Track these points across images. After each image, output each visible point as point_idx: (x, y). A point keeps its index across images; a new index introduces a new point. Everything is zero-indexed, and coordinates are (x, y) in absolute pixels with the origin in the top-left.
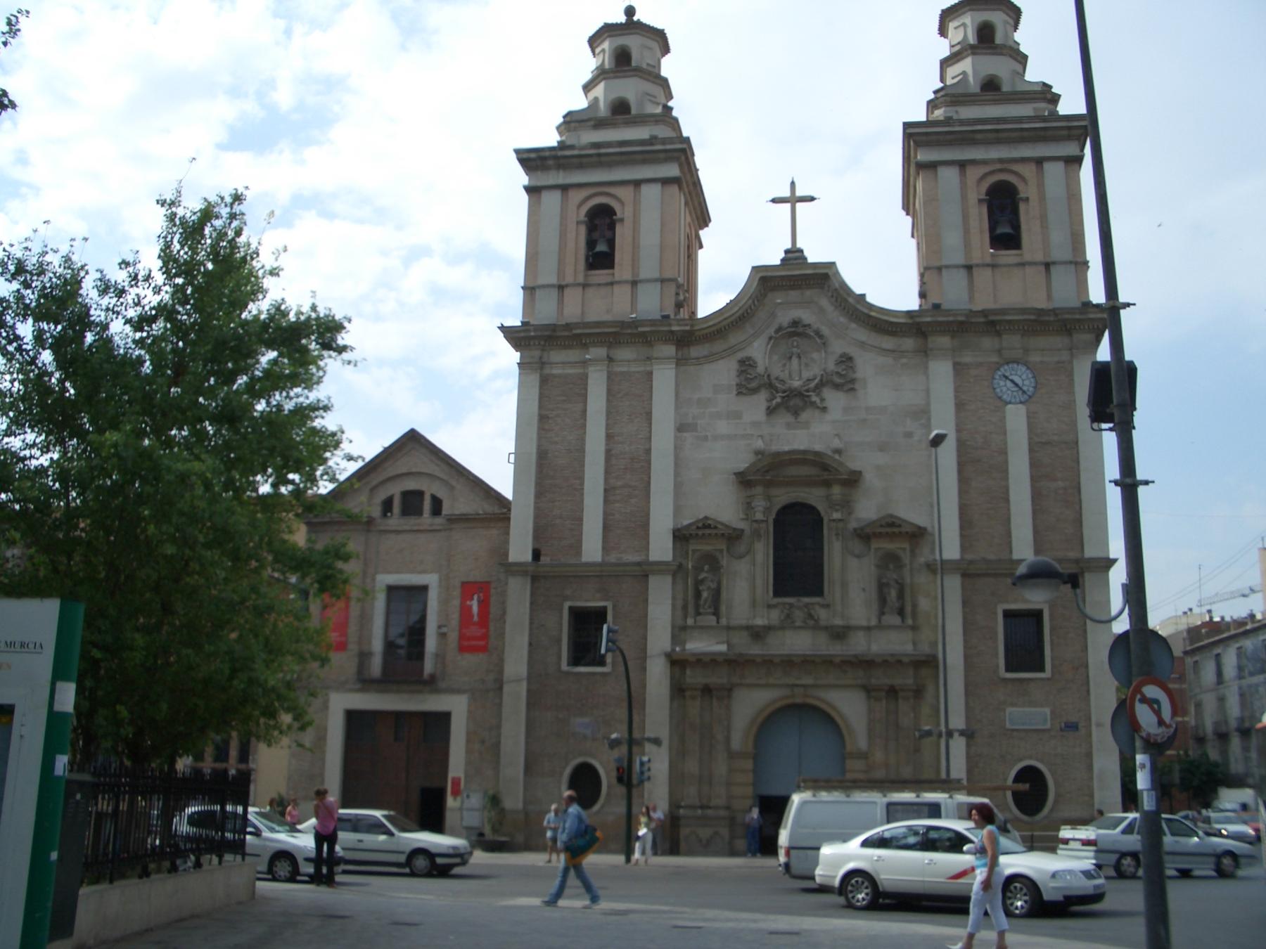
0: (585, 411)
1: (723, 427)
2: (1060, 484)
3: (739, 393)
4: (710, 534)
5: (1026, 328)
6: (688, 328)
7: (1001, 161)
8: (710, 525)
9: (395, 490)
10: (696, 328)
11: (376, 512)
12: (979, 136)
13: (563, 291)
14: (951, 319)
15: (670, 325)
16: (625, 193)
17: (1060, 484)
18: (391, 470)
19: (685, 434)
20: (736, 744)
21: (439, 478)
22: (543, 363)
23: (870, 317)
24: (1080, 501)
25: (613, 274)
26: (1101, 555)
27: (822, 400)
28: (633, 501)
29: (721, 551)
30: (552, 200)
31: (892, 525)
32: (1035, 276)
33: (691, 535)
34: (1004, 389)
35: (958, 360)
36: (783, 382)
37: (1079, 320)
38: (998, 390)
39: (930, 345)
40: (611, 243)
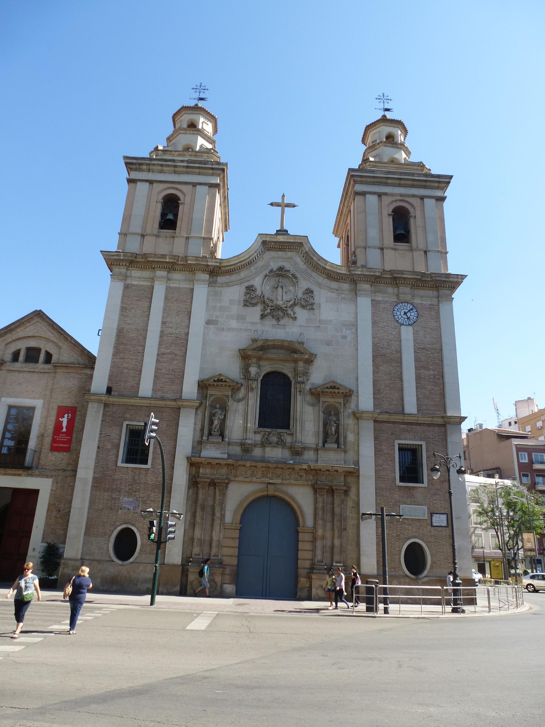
0: (150, 307)
1: (234, 324)
2: (431, 372)
3: (245, 305)
4: (222, 385)
5: (413, 283)
6: (218, 264)
7: (401, 195)
8: (222, 379)
9: (23, 346)
10: (223, 265)
11: (8, 357)
12: (390, 181)
13: (144, 238)
14: (372, 274)
15: (208, 261)
16: (186, 189)
17: (431, 372)
18: (21, 332)
19: (210, 326)
20: (228, 518)
21: (52, 341)
22: (126, 277)
23: (325, 268)
24: (443, 383)
25: (175, 233)
26: (456, 415)
27: (294, 313)
28: (175, 362)
29: (228, 396)
30: (142, 188)
31: (334, 388)
32: (418, 256)
33: (209, 385)
34: (400, 317)
35: (374, 298)
36: (272, 301)
37: (444, 281)
38: (396, 317)
39: (358, 288)
40: (176, 215)
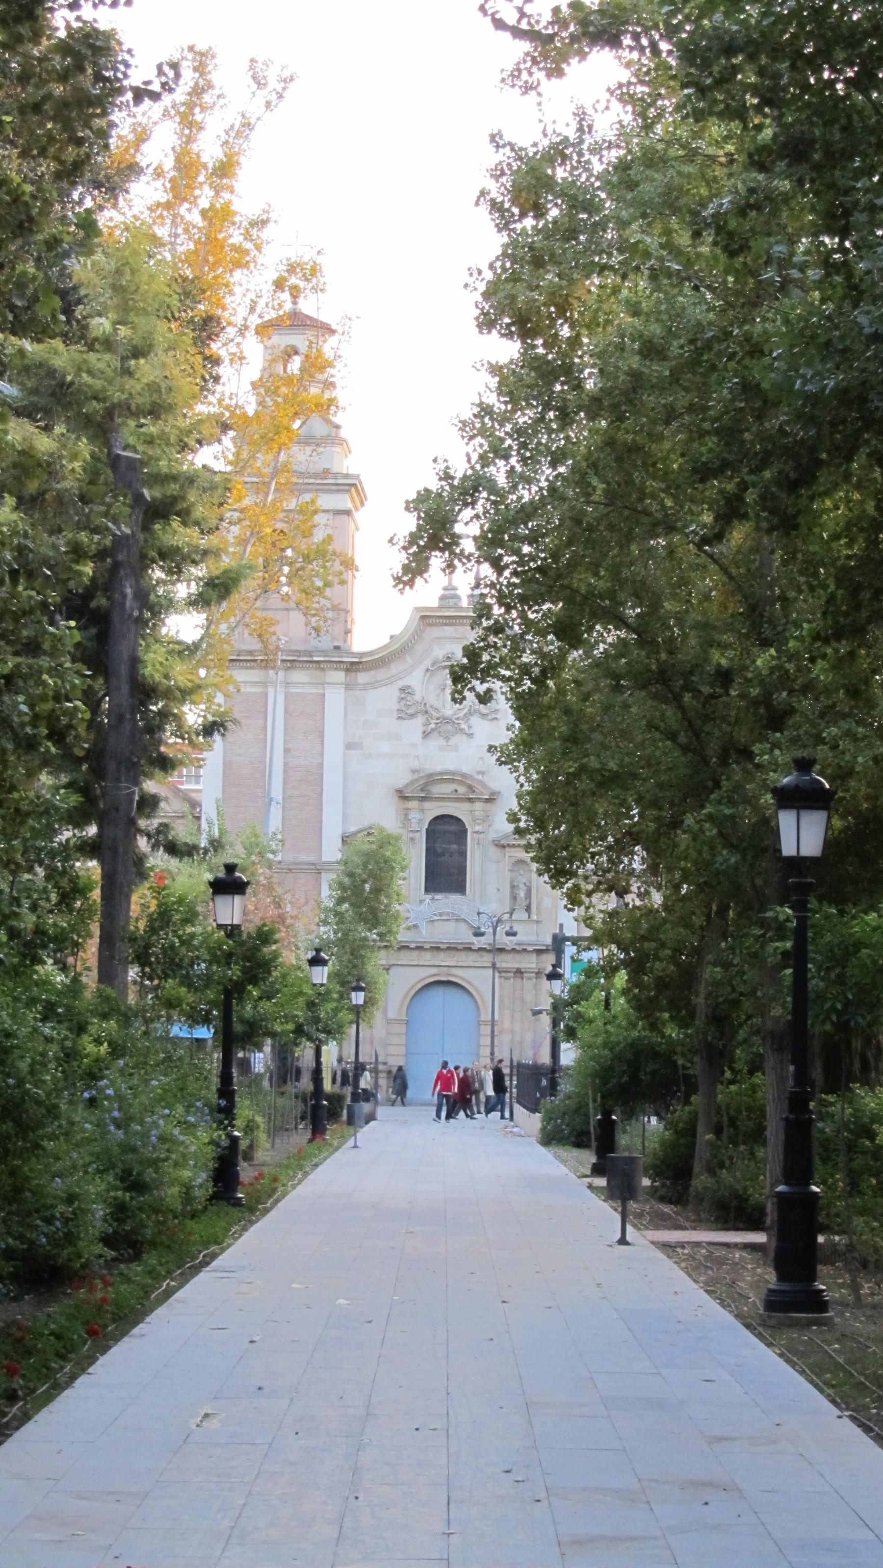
19: (352, 752)
20: (392, 1015)
27: (470, 727)
